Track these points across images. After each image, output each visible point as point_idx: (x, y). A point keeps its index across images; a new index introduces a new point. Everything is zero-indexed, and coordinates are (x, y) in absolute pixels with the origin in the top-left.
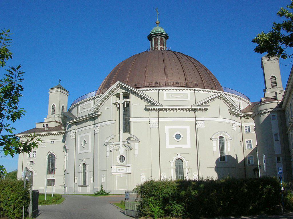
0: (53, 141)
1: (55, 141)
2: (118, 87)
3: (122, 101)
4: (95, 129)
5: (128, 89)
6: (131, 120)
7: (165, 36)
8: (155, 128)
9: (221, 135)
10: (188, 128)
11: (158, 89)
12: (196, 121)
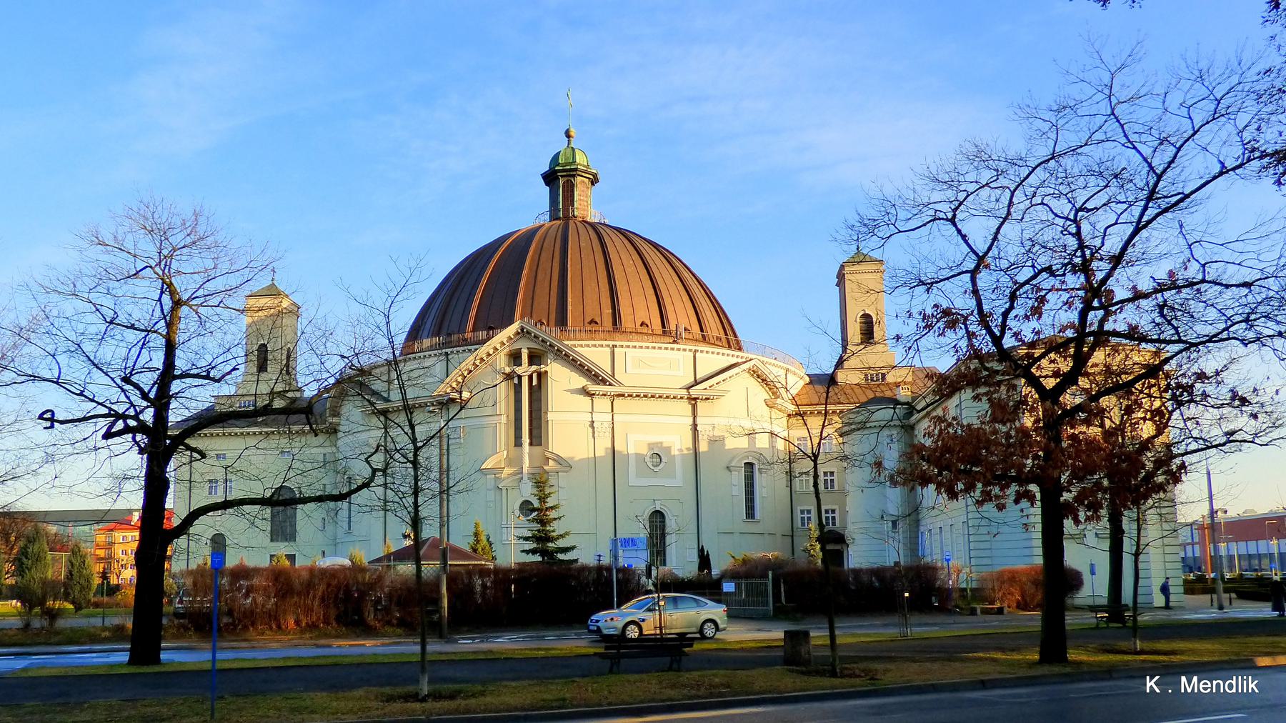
2: (517, 333)
3: (525, 369)
6: (550, 416)
7: (591, 177)
9: (750, 461)
12: (695, 426)
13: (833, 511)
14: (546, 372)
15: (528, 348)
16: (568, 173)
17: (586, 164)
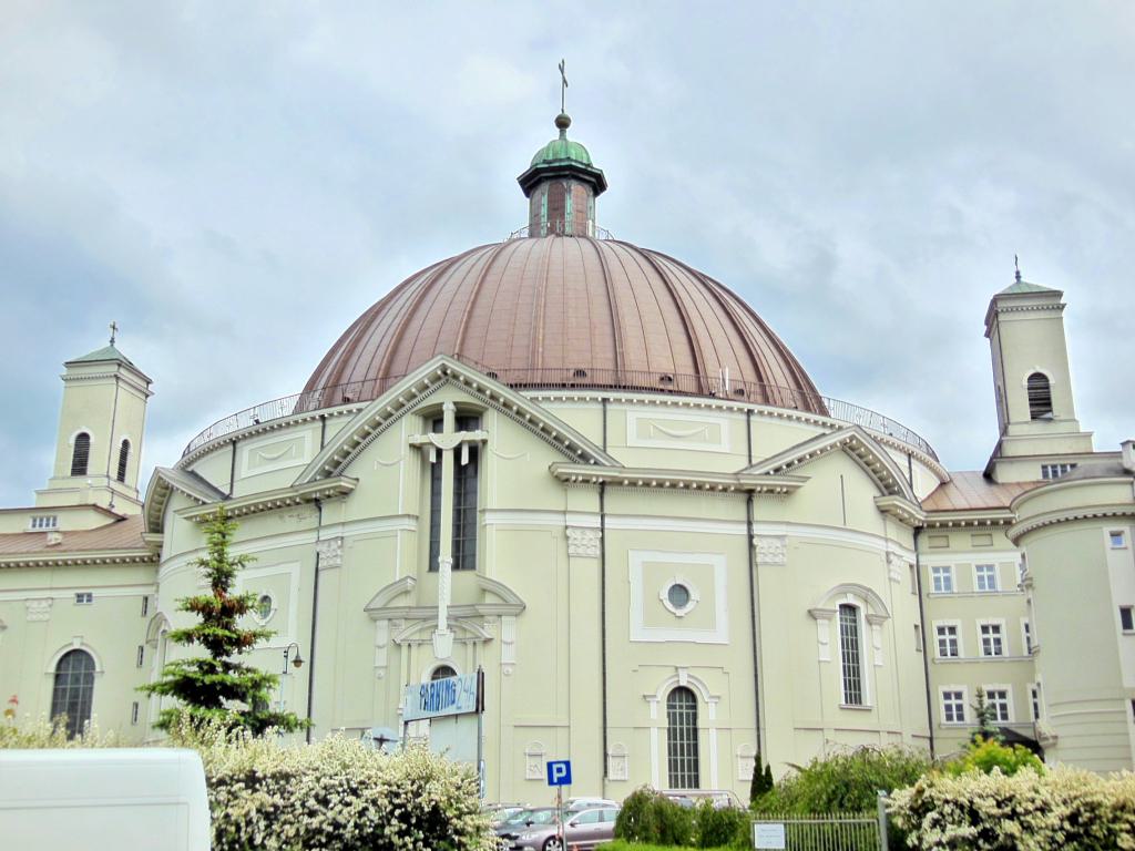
0: (90, 595)
1: (95, 593)
3: (449, 438)
4: (322, 548)
5: (480, 390)
7: (593, 180)
8: (589, 557)
9: (850, 600)
10: (719, 563)
11: (605, 401)
12: (751, 537)
13: (1002, 695)
14: (484, 442)
15: (455, 403)
16: (557, 174)
17: (585, 162)
